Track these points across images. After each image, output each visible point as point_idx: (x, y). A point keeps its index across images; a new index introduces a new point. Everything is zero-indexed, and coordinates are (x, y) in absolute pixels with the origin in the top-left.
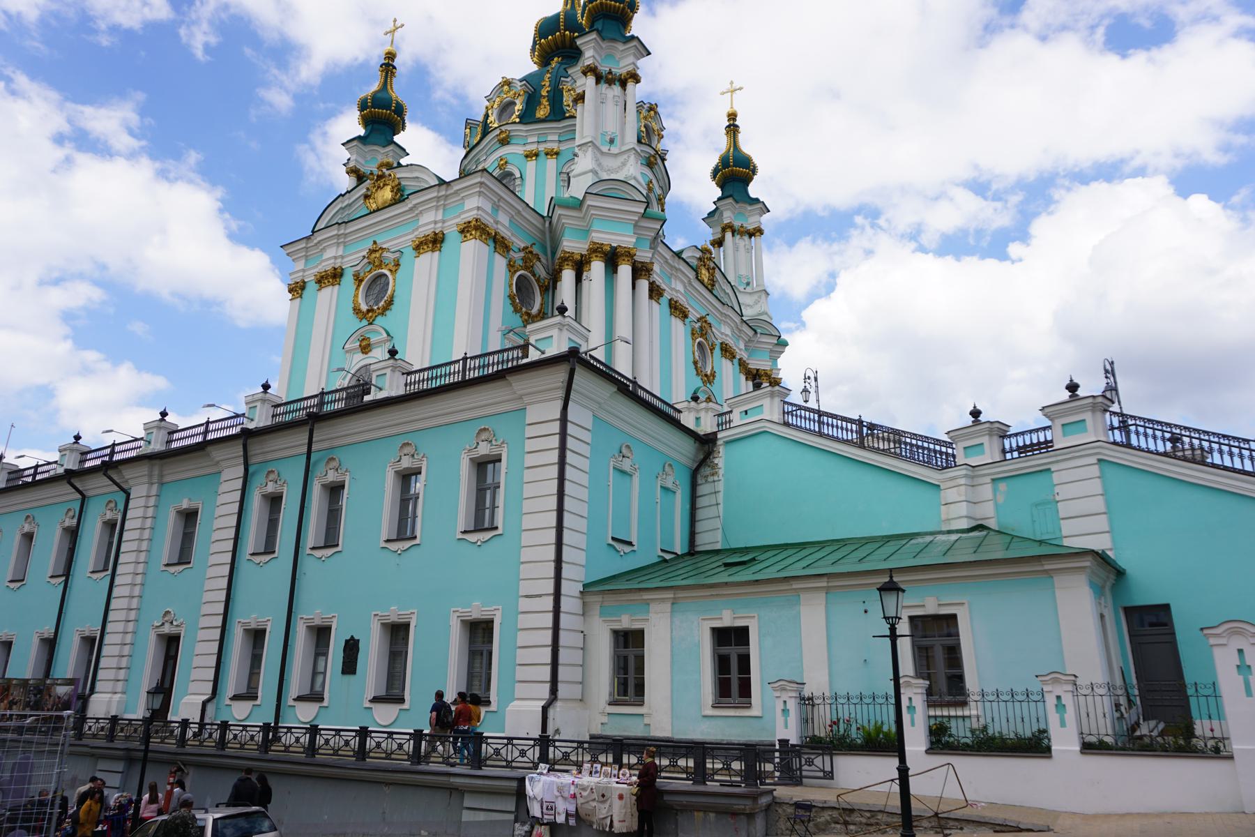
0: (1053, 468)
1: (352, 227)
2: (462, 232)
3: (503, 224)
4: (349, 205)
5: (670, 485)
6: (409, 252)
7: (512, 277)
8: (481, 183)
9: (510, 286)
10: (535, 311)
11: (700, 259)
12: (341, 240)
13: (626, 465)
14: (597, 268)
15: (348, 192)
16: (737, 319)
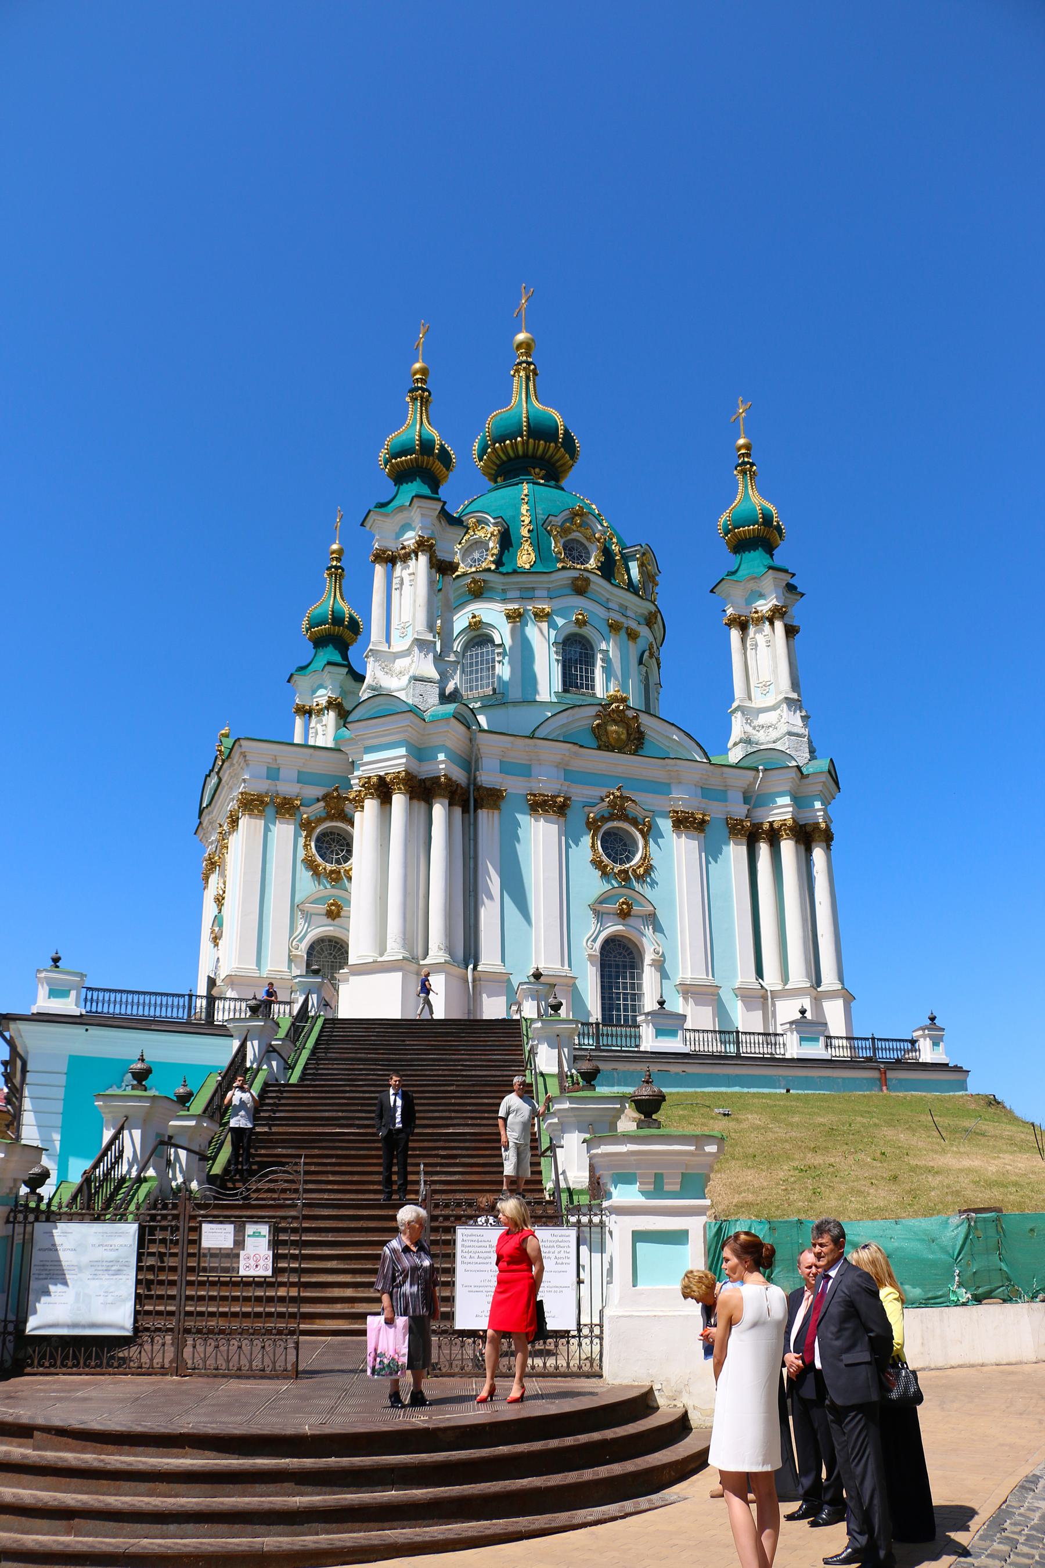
9: (306, 846)
11: (597, 716)
15: (212, 771)
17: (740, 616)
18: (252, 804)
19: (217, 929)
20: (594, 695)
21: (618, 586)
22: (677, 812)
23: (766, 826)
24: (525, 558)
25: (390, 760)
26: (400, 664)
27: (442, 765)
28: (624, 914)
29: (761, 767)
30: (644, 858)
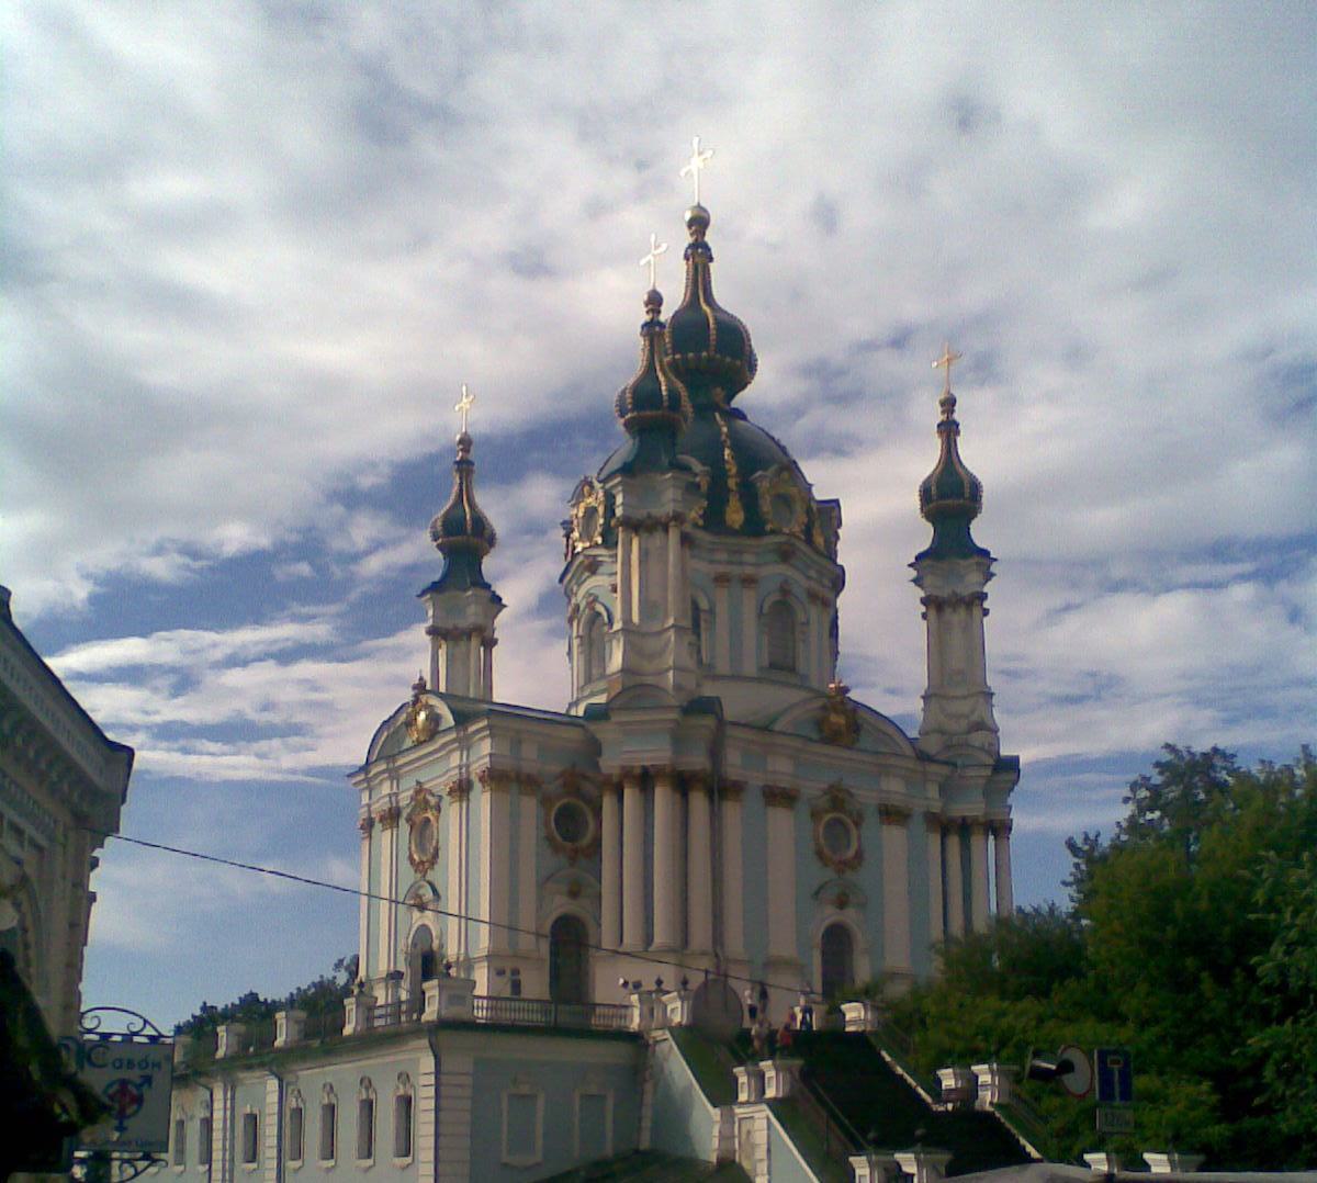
0: (756, 1115)
1: (400, 762)
2: (481, 779)
3: (530, 758)
4: (396, 732)
5: (593, 1090)
6: (447, 799)
7: (547, 814)
8: (489, 727)
9: (546, 824)
10: (585, 841)
11: (824, 708)
12: (394, 775)
13: (525, 1089)
14: (630, 795)
15: (391, 718)
16: (911, 765)
17: (937, 597)
18: (496, 778)
19: (428, 894)
20: (792, 670)
21: (817, 551)
22: (886, 806)
23: (960, 820)
24: (735, 516)
25: (654, 752)
26: (652, 644)
27: (698, 761)
28: (842, 903)
29: (959, 763)
30: (857, 853)
